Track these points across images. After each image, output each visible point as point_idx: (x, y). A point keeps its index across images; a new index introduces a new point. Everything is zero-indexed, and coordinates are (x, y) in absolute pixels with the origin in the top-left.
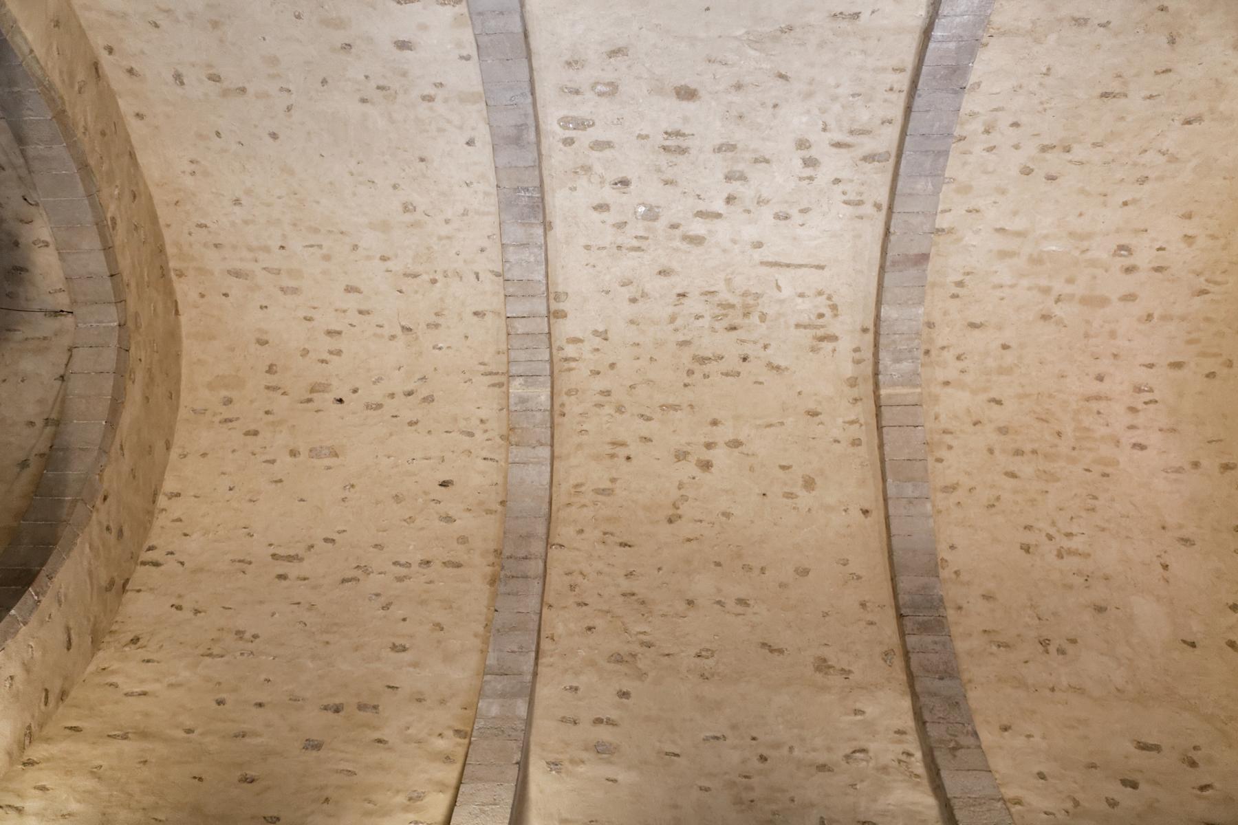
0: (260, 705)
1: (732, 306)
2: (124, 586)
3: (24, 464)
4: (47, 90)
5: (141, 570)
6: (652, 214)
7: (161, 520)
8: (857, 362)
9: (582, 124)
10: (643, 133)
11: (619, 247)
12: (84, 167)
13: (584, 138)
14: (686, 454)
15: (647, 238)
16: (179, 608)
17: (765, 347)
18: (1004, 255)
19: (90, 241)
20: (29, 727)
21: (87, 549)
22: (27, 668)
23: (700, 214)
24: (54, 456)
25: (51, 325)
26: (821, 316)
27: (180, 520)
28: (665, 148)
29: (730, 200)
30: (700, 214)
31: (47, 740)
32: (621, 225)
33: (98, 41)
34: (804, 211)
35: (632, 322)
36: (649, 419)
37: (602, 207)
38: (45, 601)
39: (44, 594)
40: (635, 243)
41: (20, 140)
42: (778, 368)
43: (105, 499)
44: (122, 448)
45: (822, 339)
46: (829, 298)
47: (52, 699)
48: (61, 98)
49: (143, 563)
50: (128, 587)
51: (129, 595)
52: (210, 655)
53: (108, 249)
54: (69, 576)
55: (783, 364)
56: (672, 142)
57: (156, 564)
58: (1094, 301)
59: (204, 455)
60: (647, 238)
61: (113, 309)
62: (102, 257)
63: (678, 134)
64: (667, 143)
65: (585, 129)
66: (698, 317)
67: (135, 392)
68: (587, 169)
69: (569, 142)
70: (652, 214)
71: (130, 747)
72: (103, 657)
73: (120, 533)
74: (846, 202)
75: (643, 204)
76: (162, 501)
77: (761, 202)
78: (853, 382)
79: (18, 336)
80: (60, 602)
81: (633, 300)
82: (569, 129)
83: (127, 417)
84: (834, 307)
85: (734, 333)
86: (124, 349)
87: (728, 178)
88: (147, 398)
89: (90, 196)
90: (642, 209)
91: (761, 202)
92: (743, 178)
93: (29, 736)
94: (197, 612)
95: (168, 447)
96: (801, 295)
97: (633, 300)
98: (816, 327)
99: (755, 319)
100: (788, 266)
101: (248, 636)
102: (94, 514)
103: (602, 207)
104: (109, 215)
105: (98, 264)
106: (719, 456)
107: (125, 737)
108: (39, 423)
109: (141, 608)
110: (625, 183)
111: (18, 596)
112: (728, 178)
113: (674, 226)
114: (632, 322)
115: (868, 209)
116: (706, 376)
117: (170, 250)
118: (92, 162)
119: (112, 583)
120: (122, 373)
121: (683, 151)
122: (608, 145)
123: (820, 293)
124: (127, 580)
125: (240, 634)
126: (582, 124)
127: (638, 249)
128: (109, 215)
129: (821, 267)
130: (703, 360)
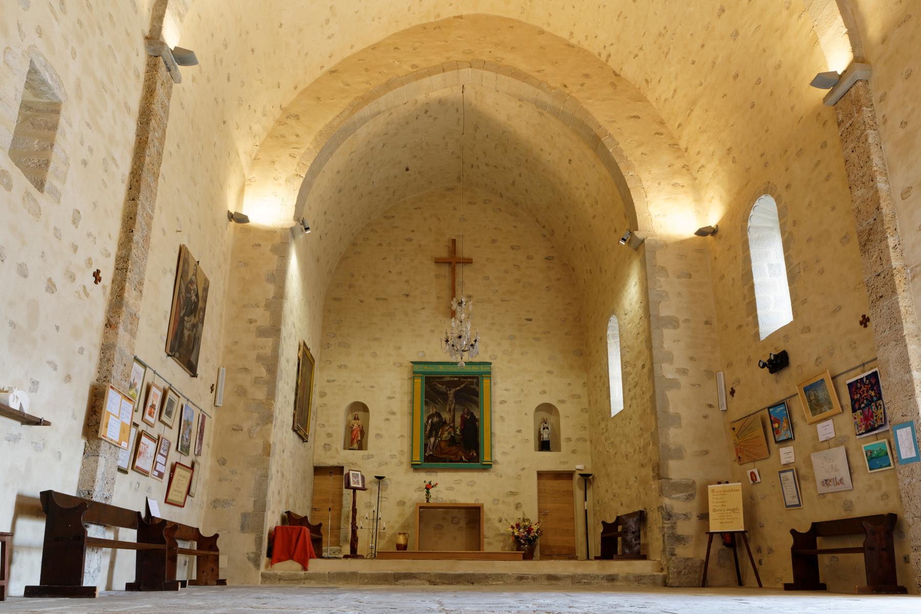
0: (703, 46)
2: (616, 75)
3: (541, 114)
4: (355, 107)
5: (609, 63)
7: (585, 45)
12: (389, 86)
16: (636, 56)
19: (426, 81)
20: (670, 145)
21: (591, 101)
22: (641, 144)
24: (540, 106)
25: (468, 90)
27: (587, 37)
31: (680, 138)
33: (318, 73)
38: (611, 131)
39: (607, 131)
41: (379, 113)
43: (565, 86)
44: (539, 71)
47: (662, 130)
48: (355, 99)
49: (607, 61)
50: (618, 72)
51: (622, 74)
52: (667, 53)
53: (429, 72)
54: (601, 113)
57: (609, 56)
59: (550, 15)
61: (462, 70)
62: (434, 77)
67: (509, 59)
71: (697, 111)
72: (651, 97)
73: (587, 76)
76: (573, 41)
79: (474, 102)
80: (613, 122)
83: (523, 67)
86: (484, 65)
88: (513, 48)
89: (402, 84)
93: (674, 146)
94: (641, 49)
95: (542, 32)
101: (663, 32)
102: (574, 95)
104: (411, 70)
105: (437, 78)
107: (692, 110)
108: (520, 103)
109: (630, 71)
111: (603, 145)
117: (424, 21)
118: (384, 81)
119: (613, 85)
120: (498, 68)
124: (614, 72)
125: (660, 35)
128: (411, 70)
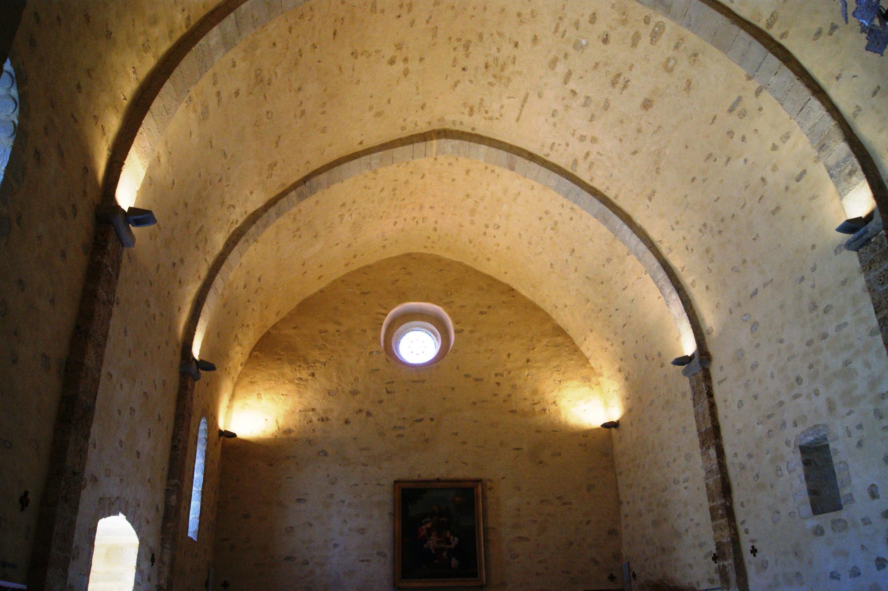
1: (502, 70)
6: (578, 46)
8: (454, 122)
9: (655, 36)
10: (634, 69)
11: (561, 18)
13: (646, 32)
14: (400, 49)
15: (563, 37)
17: (471, 81)
18: (505, 191)
23: (570, 73)
26: (487, 112)
28: (619, 75)
29: (574, 92)
30: (570, 73)
32: (577, 25)
34: (555, 125)
35: (503, 10)
36: (427, 22)
37: (593, 19)
40: (561, 29)
42: (456, 86)
45: (471, 110)
46: (497, 118)
55: (458, 89)
56: (621, 80)
58: (473, 212)
60: (563, 37)
63: (625, 87)
64: (622, 78)
65: (651, 35)
66: (498, 50)
68: (624, 22)
69: (647, 21)
70: (578, 46)
74: (553, 144)
75: (587, 45)
77: (567, 107)
78: (441, 120)
81: (519, 15)
82: (656, 26)
84: (491, 119)
85: (483, 66)
87: (587, 98)
90: (584, 42)
91: (567, 107)
92: (585, 105)
96: (502, 107)
97: (519, 15)
98: (479, 108)
99: (491, 80)
100: (523, 106)
103: (593, 19)
106: (400, 66)
110: (605, 41)
112: (587, 98)
113: (566, 56)
114: (503, 10)
115: (546, 150)
116: (455, 49)
121: (614, 83)
122: (634, 44)
123: (501, 115)
126: (655, 36)
127: (556, 30)
129: (518, 120)
130: (467, 47)
